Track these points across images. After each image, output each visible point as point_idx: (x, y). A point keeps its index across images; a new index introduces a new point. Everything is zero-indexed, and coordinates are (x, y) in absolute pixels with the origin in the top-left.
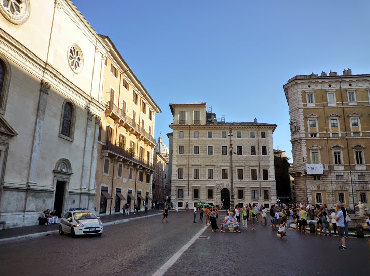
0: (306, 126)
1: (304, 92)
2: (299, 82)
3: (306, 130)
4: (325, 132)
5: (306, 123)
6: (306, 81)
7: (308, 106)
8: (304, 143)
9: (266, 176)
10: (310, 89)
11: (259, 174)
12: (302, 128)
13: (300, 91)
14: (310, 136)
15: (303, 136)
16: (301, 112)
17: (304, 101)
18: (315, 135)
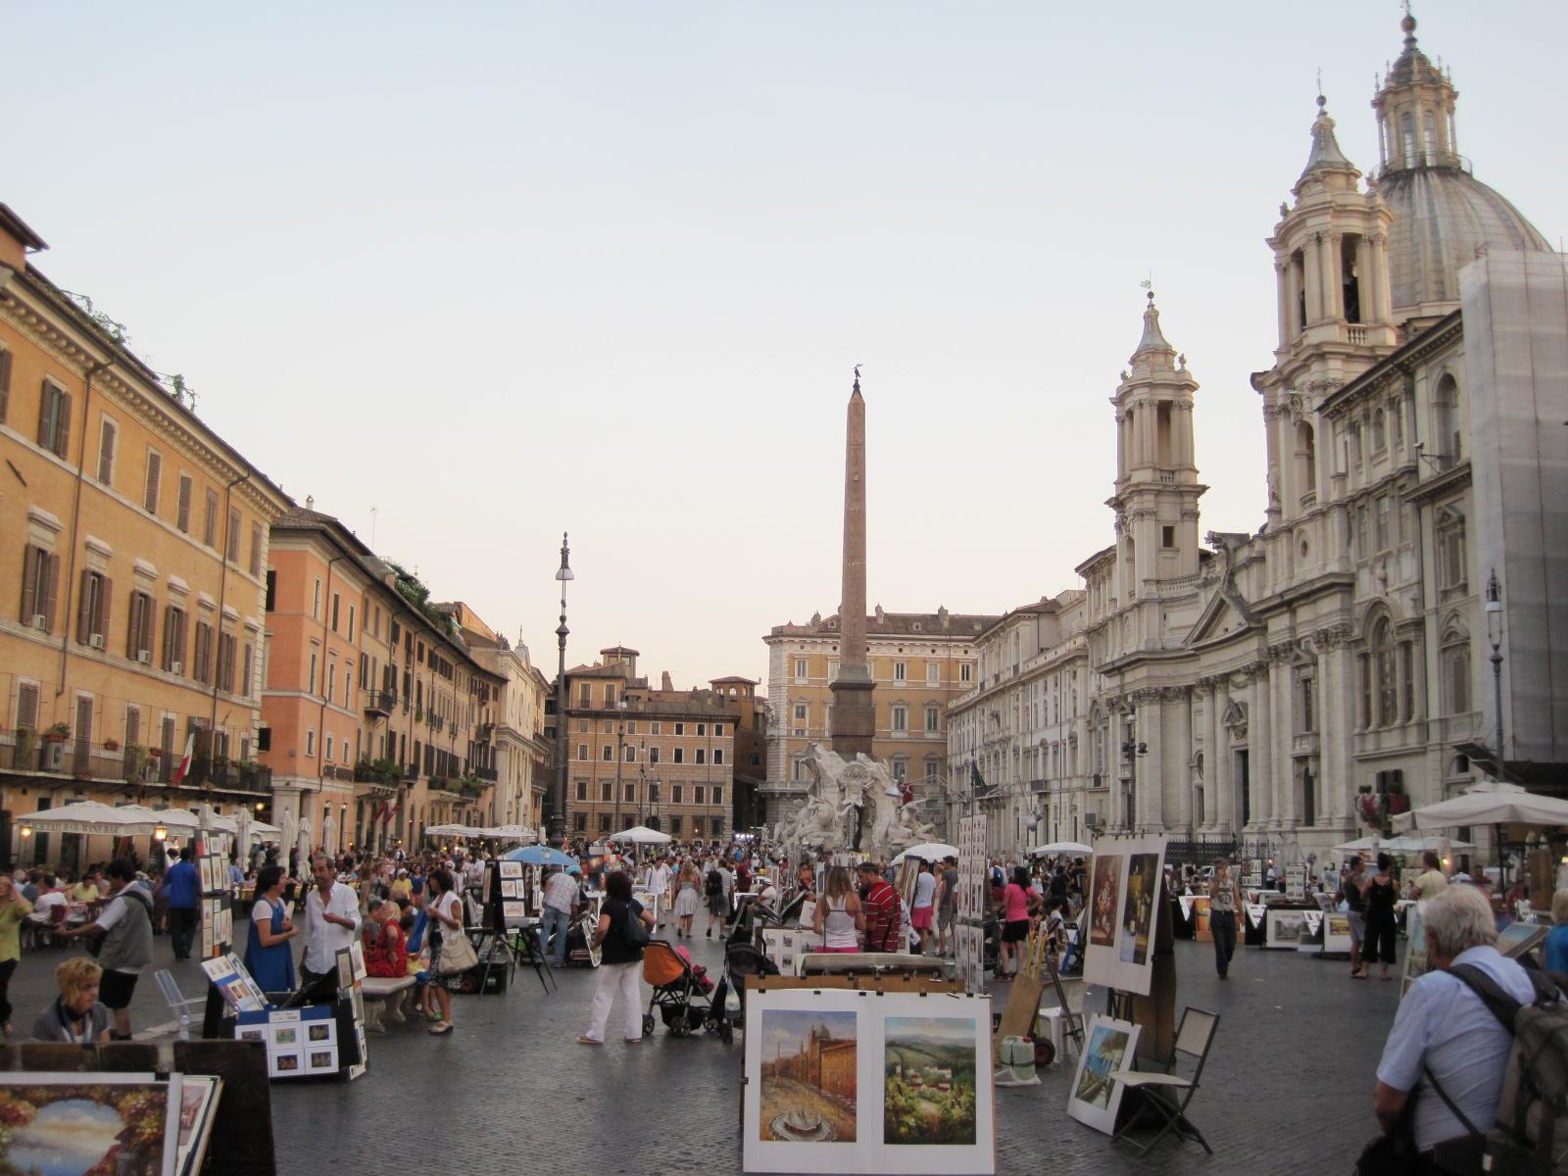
0: (789, 716)
1: (792, 658)
2: (785, 639)
3: (789, 723)
4: (817, 728)
5: (789, 711)
6: (797, 640)
7: (796, 682)
8: (783, 745)
9: (717, 799)
10: (803, 652)
11: (708, 794)
12: (783, 720)
13: (785, 654)
14: (794, 733)
15: (783, 732)
16: (784, 691)
17: (791, 672)
18: (803, 731)
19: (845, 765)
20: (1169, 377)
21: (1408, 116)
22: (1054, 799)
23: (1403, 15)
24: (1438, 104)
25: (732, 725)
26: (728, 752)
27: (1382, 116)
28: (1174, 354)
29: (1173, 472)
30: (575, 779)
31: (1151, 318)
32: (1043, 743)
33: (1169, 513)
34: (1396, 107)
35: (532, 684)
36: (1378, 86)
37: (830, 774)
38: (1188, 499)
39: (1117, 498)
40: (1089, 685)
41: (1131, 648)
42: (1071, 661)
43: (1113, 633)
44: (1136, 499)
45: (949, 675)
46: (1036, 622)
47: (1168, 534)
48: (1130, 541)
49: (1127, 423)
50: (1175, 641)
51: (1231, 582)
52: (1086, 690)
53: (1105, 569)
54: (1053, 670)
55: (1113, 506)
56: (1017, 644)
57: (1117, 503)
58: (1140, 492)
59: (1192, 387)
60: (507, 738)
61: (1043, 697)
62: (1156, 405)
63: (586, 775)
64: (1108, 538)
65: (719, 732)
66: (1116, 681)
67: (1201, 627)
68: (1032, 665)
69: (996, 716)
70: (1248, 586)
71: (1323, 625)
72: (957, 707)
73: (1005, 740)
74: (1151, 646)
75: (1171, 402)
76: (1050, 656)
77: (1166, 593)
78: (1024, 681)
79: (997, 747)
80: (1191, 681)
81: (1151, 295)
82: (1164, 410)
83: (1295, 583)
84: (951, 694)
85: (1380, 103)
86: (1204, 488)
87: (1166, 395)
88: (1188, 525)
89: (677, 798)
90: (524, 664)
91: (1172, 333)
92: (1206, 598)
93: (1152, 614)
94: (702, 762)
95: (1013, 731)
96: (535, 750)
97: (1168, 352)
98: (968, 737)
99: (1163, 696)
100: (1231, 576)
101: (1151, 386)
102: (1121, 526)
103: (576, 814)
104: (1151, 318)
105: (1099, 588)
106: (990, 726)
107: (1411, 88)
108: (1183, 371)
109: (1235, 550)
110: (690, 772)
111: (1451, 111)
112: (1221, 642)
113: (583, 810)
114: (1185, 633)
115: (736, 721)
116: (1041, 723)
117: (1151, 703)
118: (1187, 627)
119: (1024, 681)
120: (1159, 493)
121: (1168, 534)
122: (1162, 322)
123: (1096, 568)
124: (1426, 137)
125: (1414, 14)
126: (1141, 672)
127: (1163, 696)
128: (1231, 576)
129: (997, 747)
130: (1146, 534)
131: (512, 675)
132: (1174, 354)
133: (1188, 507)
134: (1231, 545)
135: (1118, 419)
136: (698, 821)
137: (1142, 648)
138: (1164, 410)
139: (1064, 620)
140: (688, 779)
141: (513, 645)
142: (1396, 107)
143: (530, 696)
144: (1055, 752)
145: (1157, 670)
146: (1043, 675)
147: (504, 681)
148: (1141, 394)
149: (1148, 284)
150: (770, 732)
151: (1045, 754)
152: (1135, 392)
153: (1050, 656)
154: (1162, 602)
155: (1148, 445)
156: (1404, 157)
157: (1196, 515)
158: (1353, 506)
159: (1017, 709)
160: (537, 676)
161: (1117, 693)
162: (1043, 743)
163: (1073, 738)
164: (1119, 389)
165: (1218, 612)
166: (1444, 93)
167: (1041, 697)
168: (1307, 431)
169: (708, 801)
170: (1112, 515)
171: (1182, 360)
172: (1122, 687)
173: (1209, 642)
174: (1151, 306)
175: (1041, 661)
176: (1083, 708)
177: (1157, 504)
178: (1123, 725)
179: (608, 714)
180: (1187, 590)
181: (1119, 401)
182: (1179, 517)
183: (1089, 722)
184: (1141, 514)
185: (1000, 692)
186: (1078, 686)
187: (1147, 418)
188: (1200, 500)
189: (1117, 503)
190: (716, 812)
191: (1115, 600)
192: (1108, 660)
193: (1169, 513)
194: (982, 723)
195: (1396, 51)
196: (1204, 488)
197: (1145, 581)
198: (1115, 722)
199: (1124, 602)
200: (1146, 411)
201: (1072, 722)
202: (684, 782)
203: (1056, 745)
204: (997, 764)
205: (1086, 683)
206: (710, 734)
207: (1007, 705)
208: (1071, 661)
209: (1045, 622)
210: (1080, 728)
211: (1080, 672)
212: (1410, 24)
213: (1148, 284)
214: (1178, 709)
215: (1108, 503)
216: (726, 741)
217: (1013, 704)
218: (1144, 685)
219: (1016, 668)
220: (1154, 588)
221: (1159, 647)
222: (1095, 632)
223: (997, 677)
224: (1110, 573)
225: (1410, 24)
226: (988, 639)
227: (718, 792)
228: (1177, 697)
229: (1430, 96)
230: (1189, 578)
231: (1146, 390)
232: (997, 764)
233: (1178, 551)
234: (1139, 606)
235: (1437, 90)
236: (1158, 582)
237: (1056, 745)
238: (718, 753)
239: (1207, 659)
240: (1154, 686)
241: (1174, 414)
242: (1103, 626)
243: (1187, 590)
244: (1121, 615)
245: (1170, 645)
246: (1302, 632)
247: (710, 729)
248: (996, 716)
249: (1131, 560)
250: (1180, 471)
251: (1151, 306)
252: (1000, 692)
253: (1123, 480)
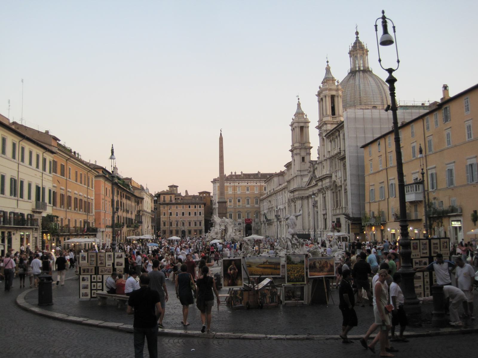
19: (221, 220)
20: (303, 120)
21: (356, 57)
22: (282, 223)
23: (356, 31)
24: (363, 54)
25: (203, 205)
26: (203, 212)
27: (350, 57)
28: (304, 114)
29: (304, 143)
30: (163, 221)
31: (299, 105)
32: (280, 209)
33: (303, 153)
34: (353, 55)
35: (150, 198)
36: (350, 49)
37: (217, 222)
38: (308, 150)
39: (291, 150)
40: (287, 195)
41: (295, 186)
42: (284, 189)
43: (292, 182)
44: (295, 150)
45: (261, 189)
46: (278, 178)
47: (303, 159)
48: (294, 160)
50: (304, 185)
51: (314, 172)
52: (288, 196)
54: (281, 190)
56: (274, 183)
57: (292, 151)
58: (296, 149)
59: (309, 122)
60: (145, 213)
61: (279, 197)
62: (300, 127)
63: (165, 220)
64: (290, 159)
65: (200, 207)
67: (308, 183)
68: (277, 189)
69: (270, 201)
70: (318, 174)
72: (262, 198)
73: (272, 208)
74: (299, 186)
75: (303, 126)
76: (281, 187)
77: (302, 174)
78: (275, 193)
79: (270, 209)
81: (299, 99)
82: (302, 128)
84: (261, 195)
85: (350, 53)
86: (312, 147)
87: (302, 125)
88: (308, 156)
89: (190, 225)
90: (148, 193)
91: (304, 109)
92: (309, 175)
93: (299, 179)
94: (196, 215)
95: (274, 206)
96: (151, 215)
97: (303, 114)
98: (265, 207)
99: (302, 198)
100: (314, 170)
101: (298, 122)
102: (292, 156)
103: (163, 230)
104: (299, 105)
106: (269, 204)
107: (357, 50)
108: (306, 118)
109: (315, 164)
110: (193, 218)
111: (367, 55)
112: (312, 186)
113: (165, 229)
114: (305, 183)
115: (205, 204)
116: (279, 204)
117: (299, 200)
118: (306, 182)
119: (275, 193)
120: (300, 149)
121: (303, 159)
122: (302, 106)
123: (288, 166)
124: (361, 62)
125: (358, 31)
126: (296, 193)
127: (302, 198)
128: (314, 170)
129: (270, 209)
130: (298, 159)
131: (145, 197)
132: (304, 114)
133: (308, 152)
134: (314, 163)
135: (291, 130)
136: (195, 231)
137: (297, 187)
138: (302, 128)
139: (285, 177)
140: (192, 220)
141: (145, 188)
142: (353, 55)
143: (150, 201)
144: (282, 211)
145: (301, 192)
146: (280, 191)
147: (143, 199)
148: (296, 125)
149: (298, 96)
150: (214, 206)
151: (280, 211)
152: (295, 124)
153: (281, 187)
154: (301, 176)
155: (298, 137)
156: (356, 67)
157: (310, 154)
159: (274, 200)
160: (151, 195)
161: (293, 197)
162: (280, 209)
163: (285, 208)
164: (292, 122)
165: (311, 180)
166: (365, 51)
167: (279, 197)
169: (198, 225)
170: (291, 153)
171: (306, 116)
172: (294, 196)
173: (311, 186)
174: (299, 102)
175: (279, 188)
176: (287, 201)
177: (300, 151)
178: (294, 205)
179: (170, 204)
180: (306, 173)
181: (292, 125)
182: (306, 154)
183: (288, 204)
184: (296, 154)
185: (271, 195)
186: (286, 195)
187: (298, 130)
188: (311, 150)
189: (292, 151)
190: (200, 228)
191: (292, 174)
192: (291, 189)
193: (303, 153)
194: (267, 203)
195: (354, 40)
196: (312, 147)
197: (297, 171)
198: (293, 204)
199: (294, 175)
200: (297, 129)
201: (285, 204)
202: (191, 221)
203: (282, 209)
204: (271, 214)
205: (288, 194)
206: (198, 208)
207: (273, 198)
208: (284, 189)
209: (281, 177)
210: (286, 205)
211: (286, 191)
212: (357, 33)
213: (298, 96)
214: (305, 202)
215: (290, 151)
216: (202, 209)
218: (297, 196)
219: (274, 189)
220: (299, 172)
221: (301, 187)
222: (289, 182)
223: (270, 191)
224: (291, 168)
225: (357, 33)
226: (268, 181)
227: (200, 223)
228: (305, 198)
229: (361, 52)
230: (308, 170)
231: (297, 123)
232: (271, 214)
233: (306, 163)
234: (296, 176)
235: (363, 50)
236: (300, 171)
237: (282, 209)
238: (200, 213)
240: (300, 196)
241: (304, 129)
243: (306, 173)
244: (293, 178)
245: (304, 186)
247: (198, 206)
248: (270, 201)
249: (295, 165)
250: (306, 143)
251: (299, 102)
252: (271, 196)
253: (293, 145)
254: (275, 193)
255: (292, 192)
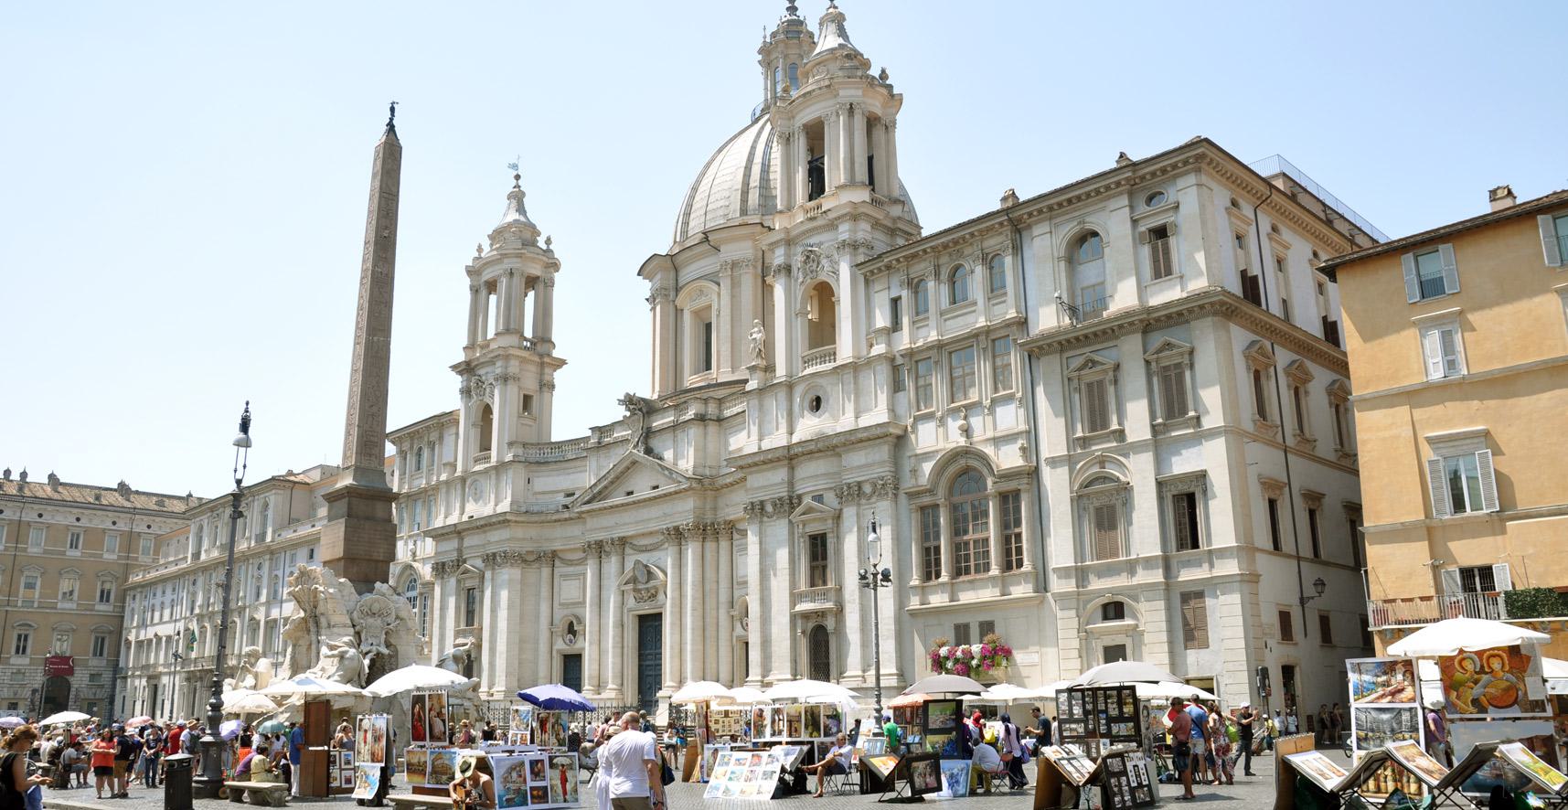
33: (530, 384)
39: (468, 363)
44: (499, 364)
48: (487, 410)
49: (484, 292)
53: (434, 436)
55: (460, 373)
57: (465, 369)
66: (454, 544)
71: (851, 478)
80: (557, 546)
83: (795, 439)
86: (562, 363)
99: (523, 560)
105: (419, 454)
158: (903, 370)
159: (259, 578)
161: (454, 556)
168: (824, 295)
170: (457, 381)
172: (460, 550)
173: (609, 502)
184: (505, 379)
189: (465, 369)
196: (562, 363)
215: (454, 367)
217: (252, 570)
224: (441, 438)
236: (524, 445)
239: (591, 523)
242: (436, 488)
244: (463, 480)
245: (536, 509)
246: (800, 489)
254: (272, 553)
255: (457, 532)
